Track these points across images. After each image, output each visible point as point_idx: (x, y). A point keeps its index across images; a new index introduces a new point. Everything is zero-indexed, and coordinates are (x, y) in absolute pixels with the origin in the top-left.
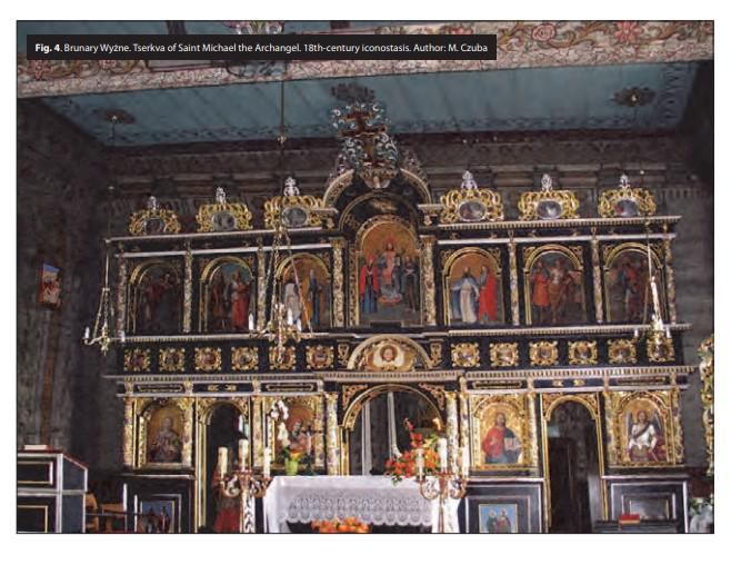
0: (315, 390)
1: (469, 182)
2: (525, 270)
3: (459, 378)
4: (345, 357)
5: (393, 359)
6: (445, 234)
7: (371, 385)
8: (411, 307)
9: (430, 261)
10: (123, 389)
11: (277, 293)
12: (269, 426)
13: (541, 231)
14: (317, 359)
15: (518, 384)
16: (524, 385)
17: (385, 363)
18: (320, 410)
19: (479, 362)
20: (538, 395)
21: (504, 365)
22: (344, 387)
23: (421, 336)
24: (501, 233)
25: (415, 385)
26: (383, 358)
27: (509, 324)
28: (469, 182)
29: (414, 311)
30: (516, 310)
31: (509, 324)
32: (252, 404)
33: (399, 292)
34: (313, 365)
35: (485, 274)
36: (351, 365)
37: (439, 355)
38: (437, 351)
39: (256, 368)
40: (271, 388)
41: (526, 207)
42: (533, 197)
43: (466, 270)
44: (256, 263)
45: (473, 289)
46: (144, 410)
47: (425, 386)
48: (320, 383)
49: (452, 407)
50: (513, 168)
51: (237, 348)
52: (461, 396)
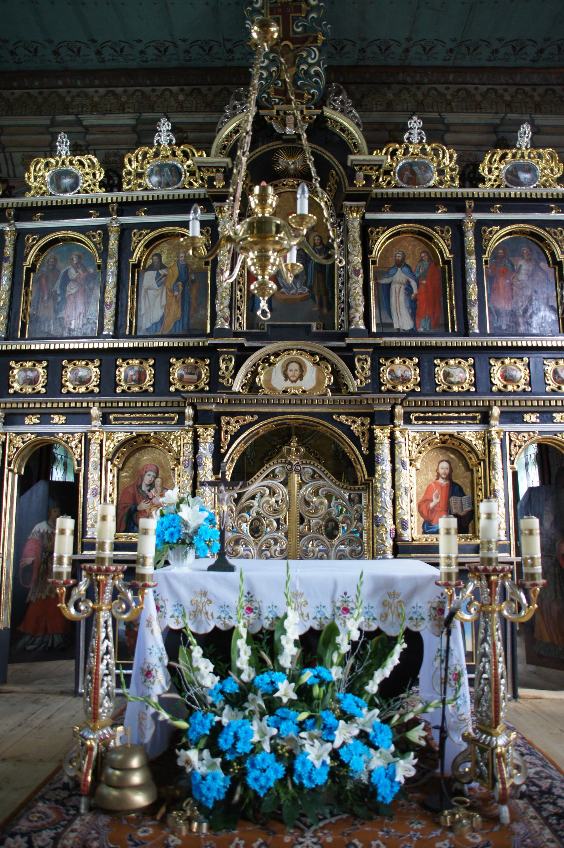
0: (181, 422)
1: (415, 132)
2: (485, 257)
3: (393, 407)
4: (228, 374)
5: (301, 377)
6: (377, 204)
7: (263, 416)
8: (321, 305)
9: (358, 239)
11: (133, 283)
12: (110, 477)
13: (510, 204)
14: (186, 377)
15: (474, 418)
16: (486, 419)
17: (288, 384)
18: (189, 449)
19: (419, 385)
20: (505, 432)
21: (455, 389)
22: (223, 418)
23: (342, 344)
24: (455, 204)
25: (328, 417)
26: (286, 377)
27: (465, 331)
28: (415, 132)
29: (325, 311)
30: (474, 312)
31: (465, 331)
32: (88, 442)
33: (305, 284)
34: (179, 386)
35: (426, 263)
36: (237, 387)
37: (369, 373)
38: (364, 366)
39: (97, 390)
40: (116, 419)
41: (490, 171)
42: (503, 157)
43: (399, 256)
44: (106, 239)
45: (408, 282)
47: (343, 418)
48: (189, 411)
49: (384, 451)
50: (473, 118)
51: (70, 361)
52: (398, 434)
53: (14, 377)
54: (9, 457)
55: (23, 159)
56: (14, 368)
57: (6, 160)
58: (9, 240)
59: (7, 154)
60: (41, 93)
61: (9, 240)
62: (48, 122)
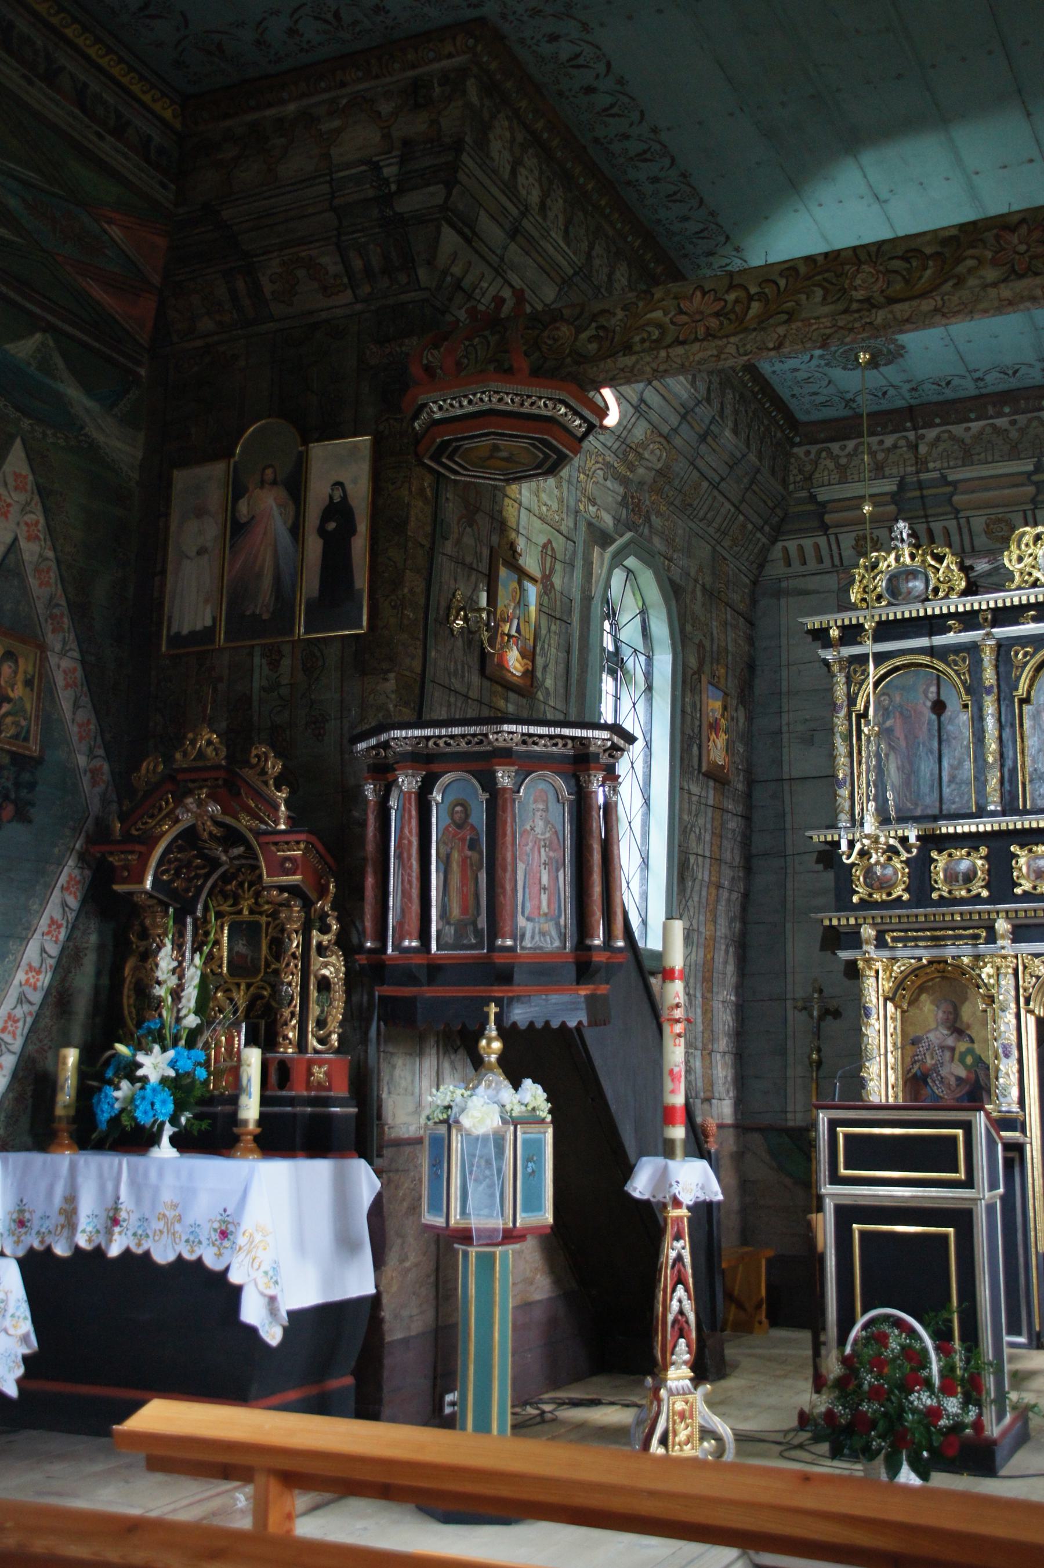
10: (854, 940)
46: (900, 984)
53: (1020, 869)
54: (1025, 990)
55: (988, 525)
56: (1018, 856)
57: (960, 528)
58: (988, 658)
59: (963, 521)
60: (1013, 423)
61: (988, 658)
62: (1031, 468)
